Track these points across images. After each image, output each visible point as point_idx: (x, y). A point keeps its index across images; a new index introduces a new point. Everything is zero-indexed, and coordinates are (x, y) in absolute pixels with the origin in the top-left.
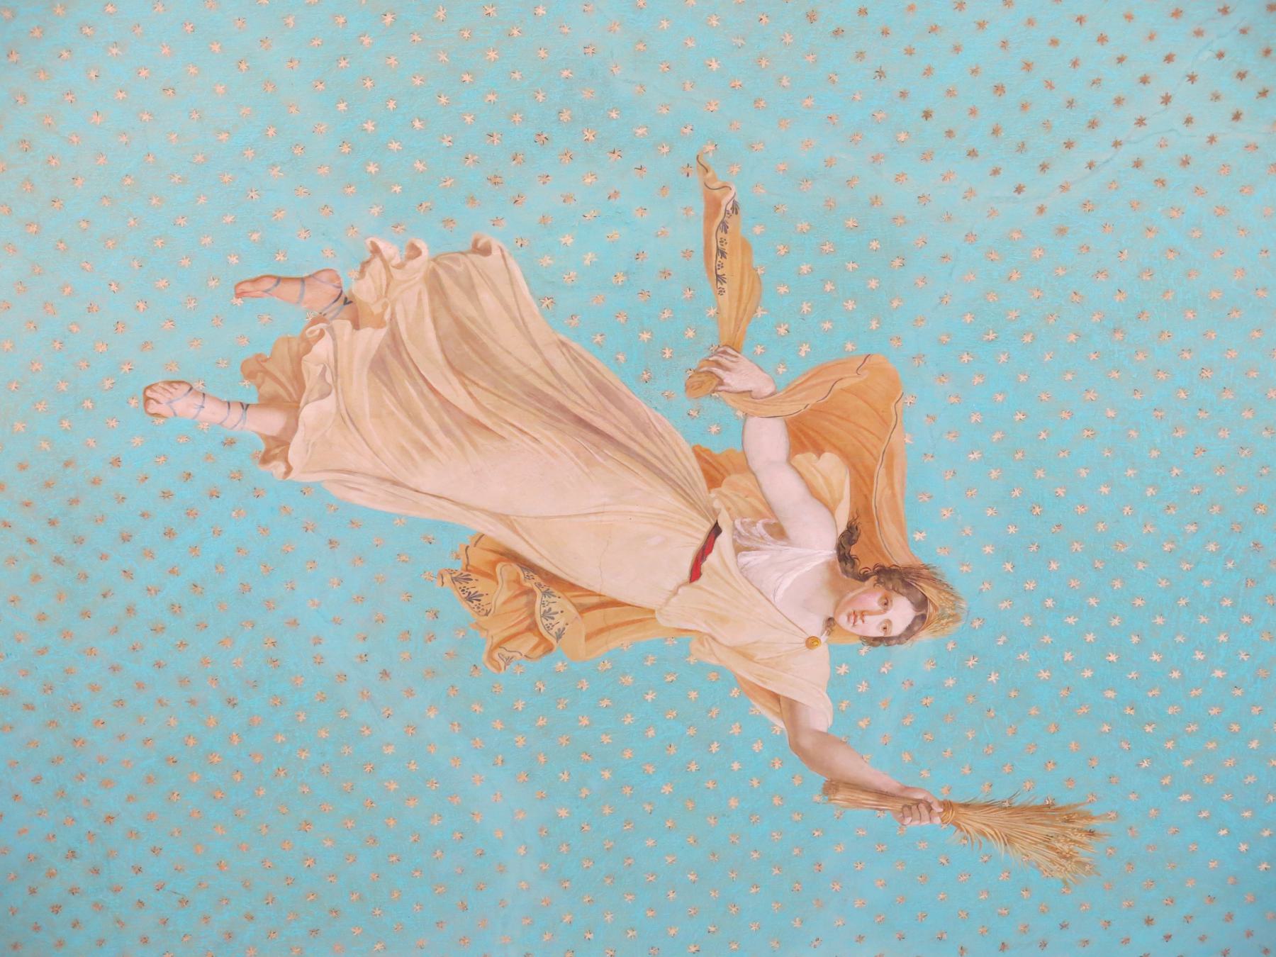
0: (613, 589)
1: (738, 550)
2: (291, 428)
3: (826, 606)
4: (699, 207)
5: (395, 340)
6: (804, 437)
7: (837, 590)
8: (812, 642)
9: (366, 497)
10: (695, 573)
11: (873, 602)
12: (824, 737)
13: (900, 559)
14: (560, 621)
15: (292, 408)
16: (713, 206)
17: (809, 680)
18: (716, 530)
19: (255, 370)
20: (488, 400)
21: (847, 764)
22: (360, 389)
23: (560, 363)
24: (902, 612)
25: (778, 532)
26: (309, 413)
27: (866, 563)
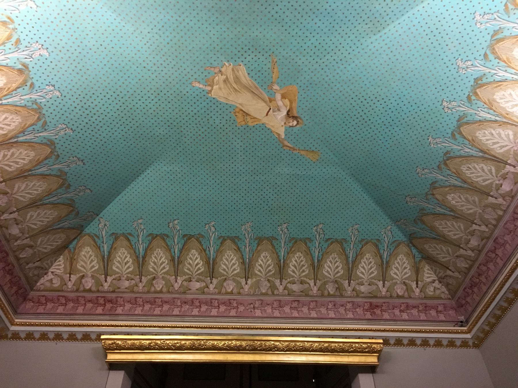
0: (255, 116)
1: (273, 112)
3: (284, 121)
5: (227, 78)
6: (283, 97)
7: (287, 119)
9: (222, 100)
10: (267, 115)
11: (291, 121)
13: (296, 115)
14: (248, 120)
15: (212, 87)
16: (273, 61)
17: (282, 132)
18: (270, 109)
20: (239, 87)
21: (286, 143)
22: (222, 85)
23: (250, 83)
24: (295, 123)
25: (279, 110)
26: (215, 87)
27: (291, 115)
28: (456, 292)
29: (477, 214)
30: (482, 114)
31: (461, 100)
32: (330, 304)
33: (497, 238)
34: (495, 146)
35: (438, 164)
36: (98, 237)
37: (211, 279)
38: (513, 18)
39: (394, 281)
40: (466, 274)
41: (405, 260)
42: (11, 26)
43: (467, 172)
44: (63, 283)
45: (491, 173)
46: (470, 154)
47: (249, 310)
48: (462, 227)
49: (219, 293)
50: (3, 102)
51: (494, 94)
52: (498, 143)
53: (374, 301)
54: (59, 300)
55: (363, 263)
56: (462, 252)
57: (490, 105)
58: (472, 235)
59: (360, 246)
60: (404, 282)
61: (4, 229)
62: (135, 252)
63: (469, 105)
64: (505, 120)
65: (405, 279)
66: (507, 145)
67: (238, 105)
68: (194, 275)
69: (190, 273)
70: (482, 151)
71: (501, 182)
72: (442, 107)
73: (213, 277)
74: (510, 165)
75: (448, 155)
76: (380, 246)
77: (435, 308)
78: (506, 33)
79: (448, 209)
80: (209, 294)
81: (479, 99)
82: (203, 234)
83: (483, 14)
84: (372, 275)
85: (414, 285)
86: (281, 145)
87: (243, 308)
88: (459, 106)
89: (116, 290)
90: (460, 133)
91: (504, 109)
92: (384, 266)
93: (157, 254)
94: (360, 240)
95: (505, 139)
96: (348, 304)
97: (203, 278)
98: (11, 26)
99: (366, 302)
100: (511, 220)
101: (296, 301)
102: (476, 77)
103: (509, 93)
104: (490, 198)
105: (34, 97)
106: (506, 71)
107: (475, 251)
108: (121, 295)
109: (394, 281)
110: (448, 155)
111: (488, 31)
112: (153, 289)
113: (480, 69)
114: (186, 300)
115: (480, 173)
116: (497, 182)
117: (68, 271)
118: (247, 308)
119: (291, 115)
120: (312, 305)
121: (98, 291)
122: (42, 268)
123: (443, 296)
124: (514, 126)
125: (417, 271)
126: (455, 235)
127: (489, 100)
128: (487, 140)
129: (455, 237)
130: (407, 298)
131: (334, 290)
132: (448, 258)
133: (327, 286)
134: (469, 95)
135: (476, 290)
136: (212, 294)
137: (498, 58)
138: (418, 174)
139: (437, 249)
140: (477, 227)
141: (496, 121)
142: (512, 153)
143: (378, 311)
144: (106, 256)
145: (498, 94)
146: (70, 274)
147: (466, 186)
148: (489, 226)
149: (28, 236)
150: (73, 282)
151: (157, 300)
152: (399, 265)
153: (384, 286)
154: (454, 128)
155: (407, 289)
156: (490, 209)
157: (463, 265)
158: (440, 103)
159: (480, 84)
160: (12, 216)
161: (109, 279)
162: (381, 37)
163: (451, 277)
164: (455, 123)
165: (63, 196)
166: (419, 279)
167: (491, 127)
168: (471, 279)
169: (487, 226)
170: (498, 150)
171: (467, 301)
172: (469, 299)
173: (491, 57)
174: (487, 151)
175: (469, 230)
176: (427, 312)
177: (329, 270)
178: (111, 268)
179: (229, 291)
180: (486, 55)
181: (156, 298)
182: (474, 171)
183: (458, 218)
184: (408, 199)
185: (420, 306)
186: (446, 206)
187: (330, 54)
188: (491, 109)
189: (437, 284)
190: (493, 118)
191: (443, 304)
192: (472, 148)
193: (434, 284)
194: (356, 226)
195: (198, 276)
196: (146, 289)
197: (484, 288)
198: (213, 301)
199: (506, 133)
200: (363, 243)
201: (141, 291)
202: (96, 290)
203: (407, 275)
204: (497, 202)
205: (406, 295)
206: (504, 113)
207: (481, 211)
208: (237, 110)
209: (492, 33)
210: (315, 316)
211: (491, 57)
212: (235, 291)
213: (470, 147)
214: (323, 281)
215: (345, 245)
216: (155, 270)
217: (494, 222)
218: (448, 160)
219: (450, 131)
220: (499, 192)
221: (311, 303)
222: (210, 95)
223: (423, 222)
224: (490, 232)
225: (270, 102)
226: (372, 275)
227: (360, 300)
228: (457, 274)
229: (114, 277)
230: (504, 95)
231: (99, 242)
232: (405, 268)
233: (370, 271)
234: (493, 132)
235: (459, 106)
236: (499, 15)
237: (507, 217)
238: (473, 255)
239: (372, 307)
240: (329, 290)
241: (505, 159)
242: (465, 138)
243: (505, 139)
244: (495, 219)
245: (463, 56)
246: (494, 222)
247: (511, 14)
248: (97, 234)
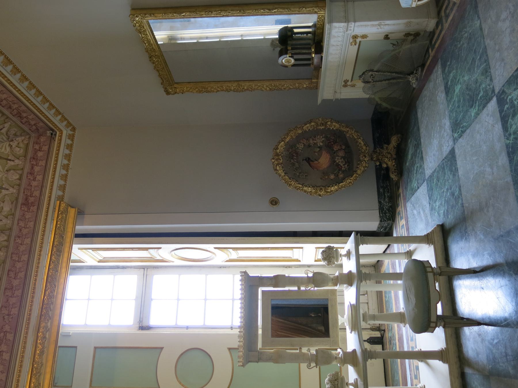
28: (24, 131)
39: (4, 179)
40: (8, 118)
47: (10, 320)
53: (20, 201)
60: (7, 171)
77: (36, 151)
85: (11, 163)
87: (7, 326)
99: (21, 208)
101: (8, 273)
109: (4, 179)
118: (7, 322)
120: (15, 258)
123: (26, 142)
130: (23, 172)
131: (3, 235)
135: (24, 115)
143: (31, 200)
153: (7, 189)
155: (14, 170)
163: (8, 131)
166: (6, 157)
168: (13, 116)
171: (34, 124)
172: (32, 123)
176: (39, 158)
185: (32, 163)
189: (14, 144)
191: (34, 143)
193: (14, 146)
197: (23, 108)
205: (20, 172)
210: (27, 256)
221: (14, 258)
228: (7, 125)
239: (26, 203)
240: (2, 239)
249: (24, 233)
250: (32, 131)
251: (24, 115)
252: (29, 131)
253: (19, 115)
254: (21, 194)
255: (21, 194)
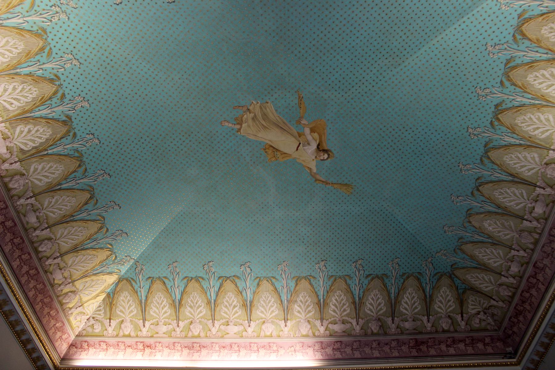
0: (286, 151)
2: (241, 128)
3: (315, 155)
4: (297, 97)
5: (255, 116)
6: (312, 130)
8: (313, 160)
9: (252, 138)
10: (297, 150)
11: (322, 154)
12: (315, 173)
13: (326, 148)
15: (241, 125)
16: (299, 97)
17: (313, 165)
18: (300, 144)
19: (236, 119)
21: (318, 177)
22: (250, 122)
24: (326, 156)
25: (309, 144)
26: (243, 125)
27: (321, 149)
28: (501, 323)
29: (514, 239)
30: (507, 138)
31: (485, 127)
32: (374, 344)
33: (536, 263)
34: (523, 169)
35: (471, 190)
36: (136, 282)
37: (249, 323)
38: (522, 47)
39: (439, 315)
40: (510, 303)
41: (448, 293)
42: (57, 83)
43: (500, 197)
44: (104, 329)
45: (523, 197)
46: (501, 179)
48: (501, 254)
49: (258, 337)
50: (49, 152)
51: (515, 119)
52: (525, 166)
53: (419, 337)
54: (100, 345)
55: (406, 298)
56: (504, 279)
57: (513, 130)
58: (512, 261)
59: (402, 281)
60: (449, 316)
61: (48, 273)
62: (171, 295)
63: (493, 131)
64: (529, 144)
65: (450, 312)
66: (534, 168)
67: (267, 142)
68: (232, 319)
69: (228, 317)
70: (511, 175)
71: (533, 204)
72: (468, 133)
73: (251, 320)
74: (540, 187)
75: (480, 181)
76: (422, 280)
77: (482, 340)
78: (518, 61)
79: (486, 236)
80: (247, 337)
81: (502, 124)
82: (238, 275)
83: (494, 45)
84: (416, 311)
85: (459, 318)
86: (314, 179)
88: (484, 132)
89: (154, 336)
90: (489, 158)
91: (526, 132)
92: (428, 300)
93: (193, 297)
94: (401, 274)
95: (532, 161)
96: (393, 342)
97: (241, 321)
98: (57, 83)
99: (412, 339)
100: (548, 243)
101: (338, 341)
102: (495, 104)
103: (528, 117)
104: (525, 222)
105: (76, 146)
106: (523, 96)
107: (517, 278)
108: (159, 340)
109: (439, 315)
110: (480, 181)
111: (501, 60)
112: (190, 334)
113: (498, 97)
114: (224, 345)
115: (512, 197)
116: (530, 205)
117: (108, 317)
119: (321, 149)
121: (137, 336)
122: (84, 313)
123: (489, 327)
124: (538, 149)
125: (461, 302)
126: (495, 262)
127: (511, 125)
128: (515, 164)
129: (496, 265)
130: (452, 332)
131: (378, 328)
132: (491, 288)
133: (370, 324)
134: (492, 121)
135: (521, 318)
136: (251, 338)
137: (514, 84)
138: (453, 201)
139: (479, 278)
140: (516, 253)
141: (520, 145)
142: (540, 175)
143: (424, 348)
144: (143, 301)
145: (520, 119)
146: (110, 319)
147: (500, 211)
148: (528, 251)
149: (70, 281)
150: (113, 327)
151: (195, 345)
152: (443, 298)
153: (428, 321)
154: (482, 154)
155: (452, 323)
156: (526, 233)
157: (505, 293)
158: (466, 130)
159: (500, 110)
160: (56, 261)
161: (147, 324)
162: (401, 70)
163: (495, 307)
164: (482, 149)
165: (102, 240)
166: (464, 311)
167: (516, 151)
168: (515, 308)
169: (525, 251)
170: (527, 174)
171: (514, 332)
172: (515, 329)
173: (507, 83)
174: (516, 175)
175: (508, 257)
176: (474, 345)
177: (371, 307)
178: (149, 312)
179: (268, 334)
180: (502, 83)
181: (193, 343)
182: (506, 195)
183: (496, 244)
184: (446, 228)
185: (467, 339)
186: (483, 233)
187: (355, 88)
188: (514, 133)
189: (482, 316)
190: (518, 142)
191: (490, 336)
192: (502, 173)
193: (479, 316)
194: (397, 260)
195: (236, 320)
196: (184, 334)
197: (529, 316)
198: (252, 345)
199: (532, 156)
200: (405, 277)
201: (179, 336)
202: (135, 335)
203: (451, 309)
204: (531, 225)
205: (452, 329)
206: (526, 136)
207: (518, 236)
208: (267, 147)
209: (505, 62)
210: (359, 356)
211: (507, 83)
212: (275, 334)
213: (500, 171)
214: (366, 319)
215: (386, 281)
216: (192, 314)
217: (531, 246)
218: (480, 186)
219: (478, 157)
220: (533, 215)
222: (239, 133)
223: (463, 252)
224: (529, 257)
225: (300, 137)
226: (416, 311)
227: (404, 337)
228: (501, 304)
229: (151, 322)
230: (524, 119)
231: (136, 287)
232: (449, 301)
233: (414, 306)
234: (520, 156)
235: (484, 132)
236: (509, 45)
237: (543, 240)
238: (515, 282)
239: (418, 344)
240: (373, 328)
241: (534, 182)
242: (493, 163)
243: (532, 161)
244: (531, 243)
245: (481, 84)
246: (531, 246)
247: (520, 44)
248: (135, 278)
249: (384, 348)
250: (504, 331)
251: (521, 318)
252: (503, 328)
253: (518, 313)
254: (428, 336)
255: (428, 336)
